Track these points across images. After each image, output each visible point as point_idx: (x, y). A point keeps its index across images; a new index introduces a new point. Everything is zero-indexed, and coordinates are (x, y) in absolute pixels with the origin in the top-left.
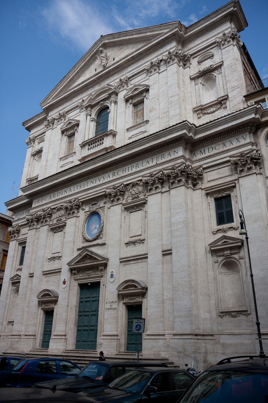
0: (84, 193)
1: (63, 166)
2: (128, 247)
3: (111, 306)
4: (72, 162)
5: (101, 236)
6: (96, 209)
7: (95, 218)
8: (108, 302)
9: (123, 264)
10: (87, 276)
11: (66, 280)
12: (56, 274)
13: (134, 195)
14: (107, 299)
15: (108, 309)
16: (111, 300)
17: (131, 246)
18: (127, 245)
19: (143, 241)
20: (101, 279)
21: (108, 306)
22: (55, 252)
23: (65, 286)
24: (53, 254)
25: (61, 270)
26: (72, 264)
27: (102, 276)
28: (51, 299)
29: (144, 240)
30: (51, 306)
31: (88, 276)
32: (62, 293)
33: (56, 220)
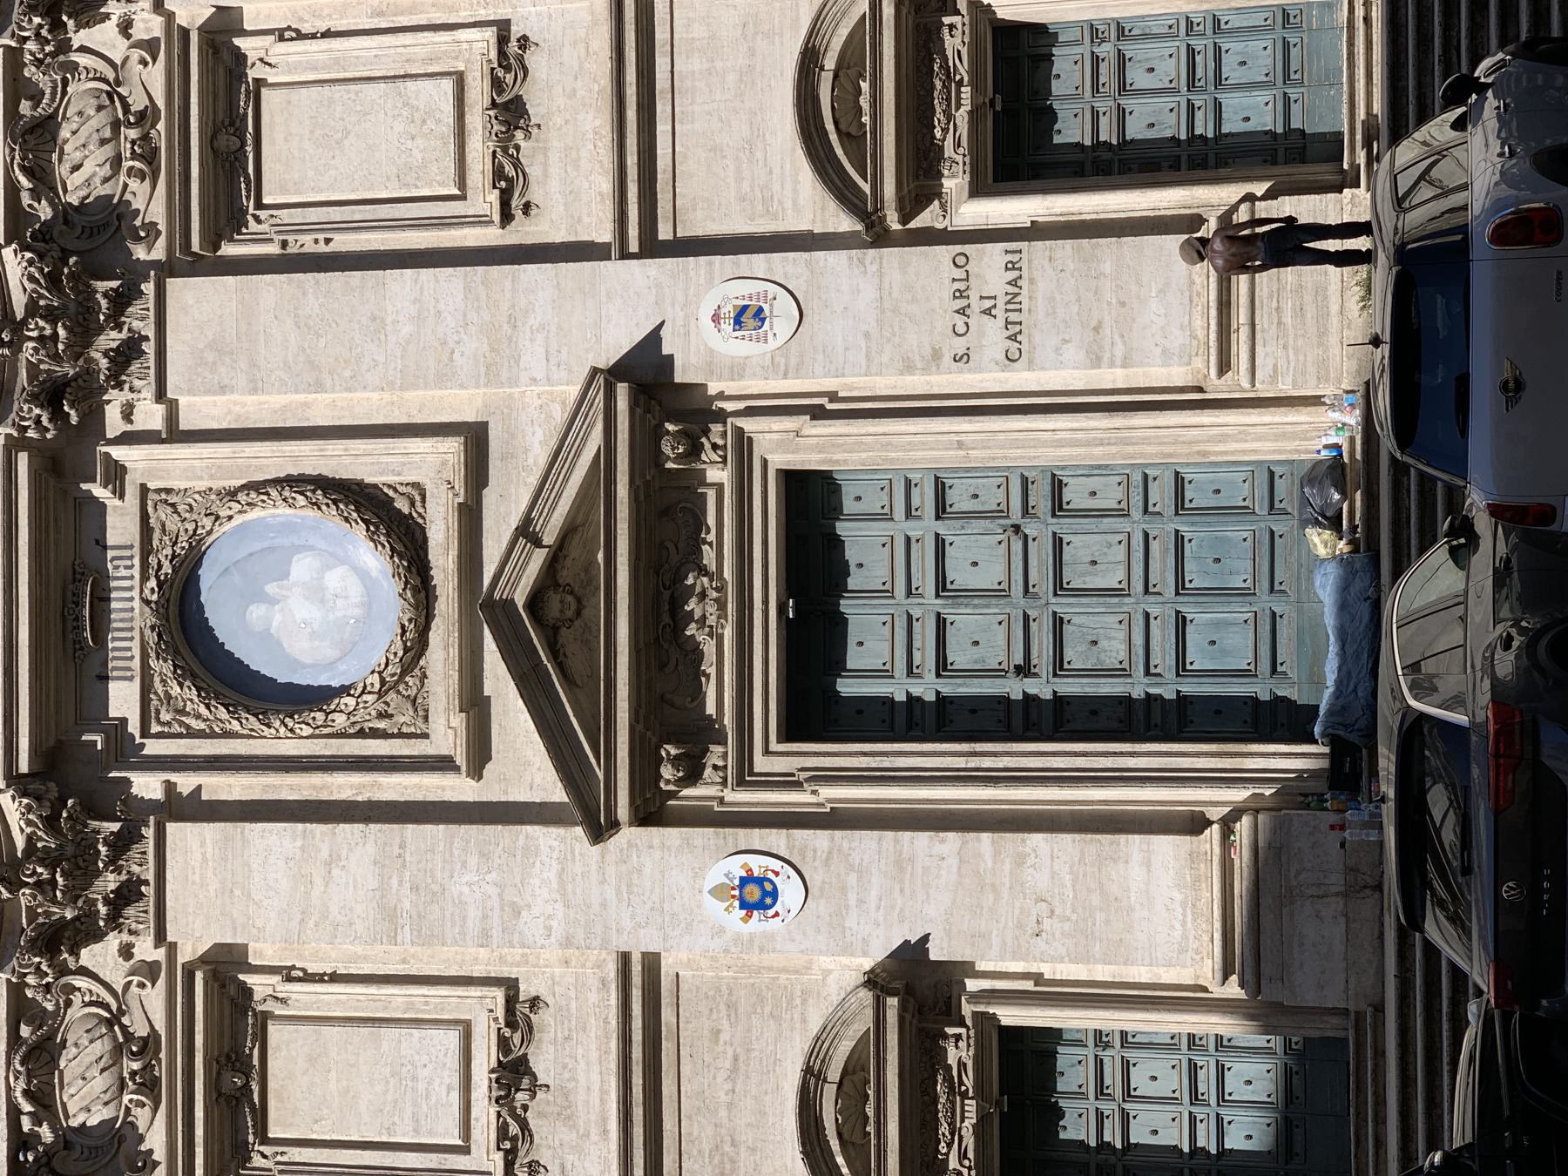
2: (534, 196)
3: (987, 312)
6: (144, 578)
8: (959, 345)
10: (722, 615)
12: (667, 1046)
13: (116, 162)
15: (1013, 338)
16: (946, 316)
17: (533, 171)
19: (513, 47)
20: (765, 463)
21: (992, 334)
22: (455, 1097)
23: (790, 891)
25: (636, 960)
27: (743, 444)
29: (503, 40)
30: (962, 1065)
31: (721, 605)
32: (851, 922)
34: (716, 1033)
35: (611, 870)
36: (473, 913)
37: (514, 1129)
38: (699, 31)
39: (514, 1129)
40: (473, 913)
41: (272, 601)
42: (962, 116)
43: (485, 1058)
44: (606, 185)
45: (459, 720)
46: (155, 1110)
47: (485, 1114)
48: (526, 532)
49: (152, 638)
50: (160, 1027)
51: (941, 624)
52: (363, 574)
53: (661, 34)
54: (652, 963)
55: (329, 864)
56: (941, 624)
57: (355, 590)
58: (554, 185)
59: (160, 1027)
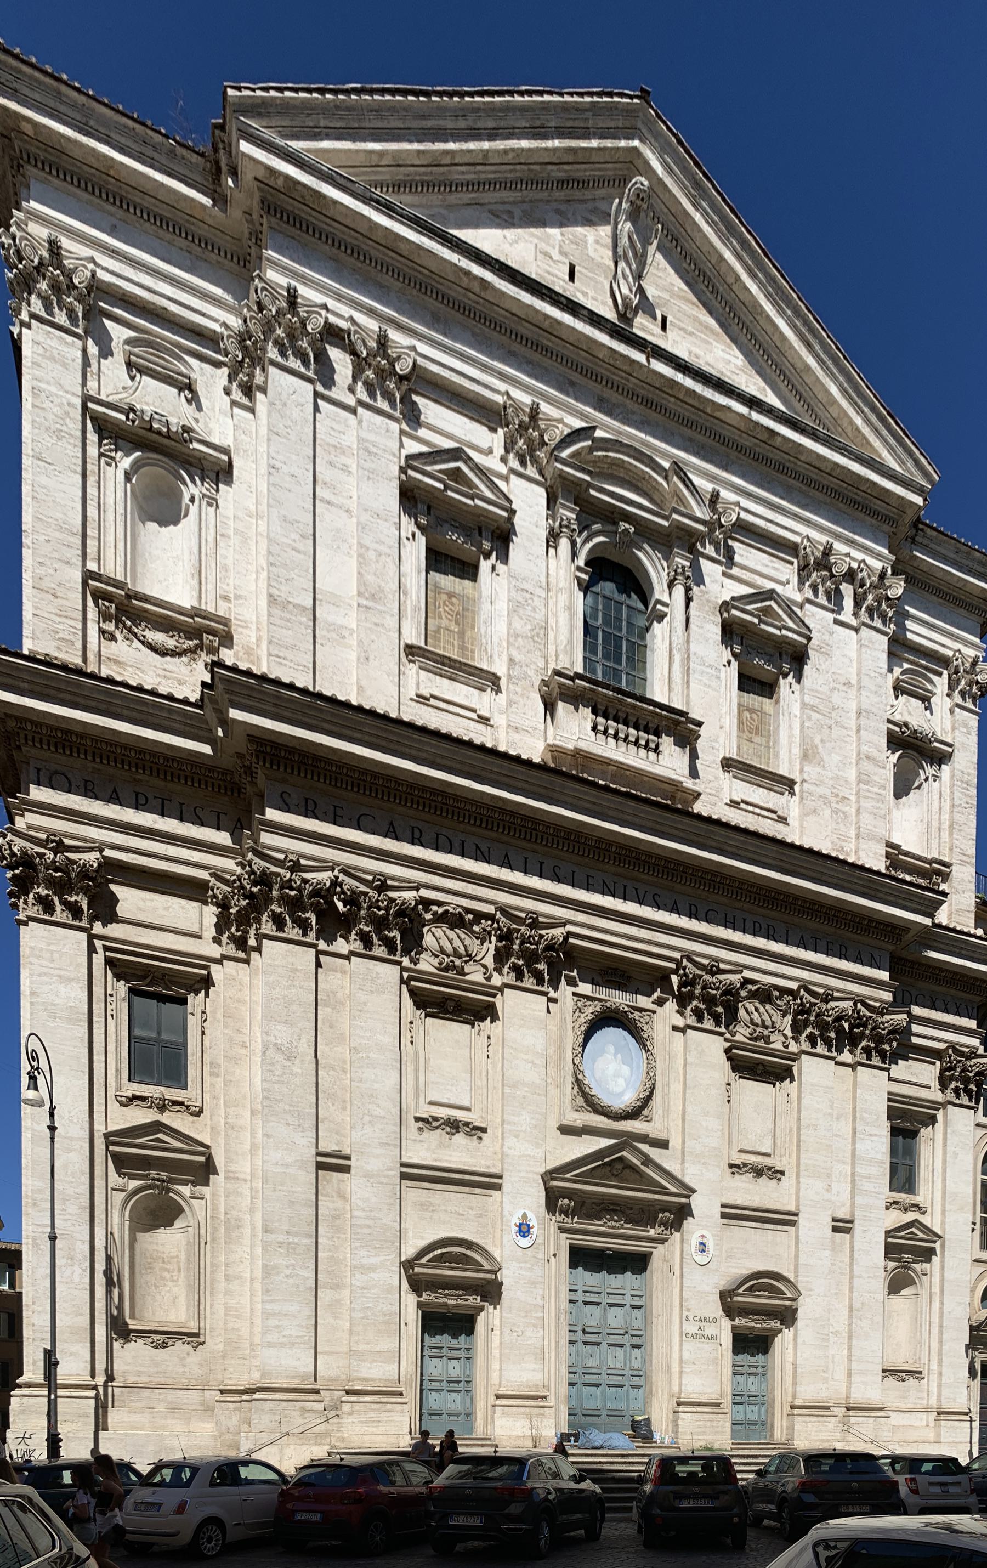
0: (581, 917)
1: (432, 702)
4: (484, 720)
5: (645, 1112)
6: (628, 1006)
7: (610, 1036)
8: (691, 1318)
9: (725, 1221)
11: (533, 1222)
12: (467, 1189)
14: (688, 1310)
18: (734, 1170)
21: (692, 1328)
22: (445, 1101)
24: (431, 1103)
26: (568, 1176)
28: (481, 1275)
32: (514, 1263)
33: (436, 962)
34: (471, 1208)
35: (531, 1175)
36: (516, 1119)
37: (437, 1124)
38: (778, 1239)
39: (437, 1124)
40: (516, 1119)
41: (615, 1055)
42: (752, 1324)
43: (461, 1115)
44: (739, 1202)
45: (579, 1124)
46: (438, 969)
47: (443, 1113)
48: (647, 1161)
49: (608, 1004)
50: (467, 978)
51: (598, 1304)
52: (622, 1094)
53: (779, 1227)
54: (498, 1187)
55: (532, 1062)
56: (598, 1304)
57: (618, 1090)
58: (740, 1184)
59: (467, 978)
